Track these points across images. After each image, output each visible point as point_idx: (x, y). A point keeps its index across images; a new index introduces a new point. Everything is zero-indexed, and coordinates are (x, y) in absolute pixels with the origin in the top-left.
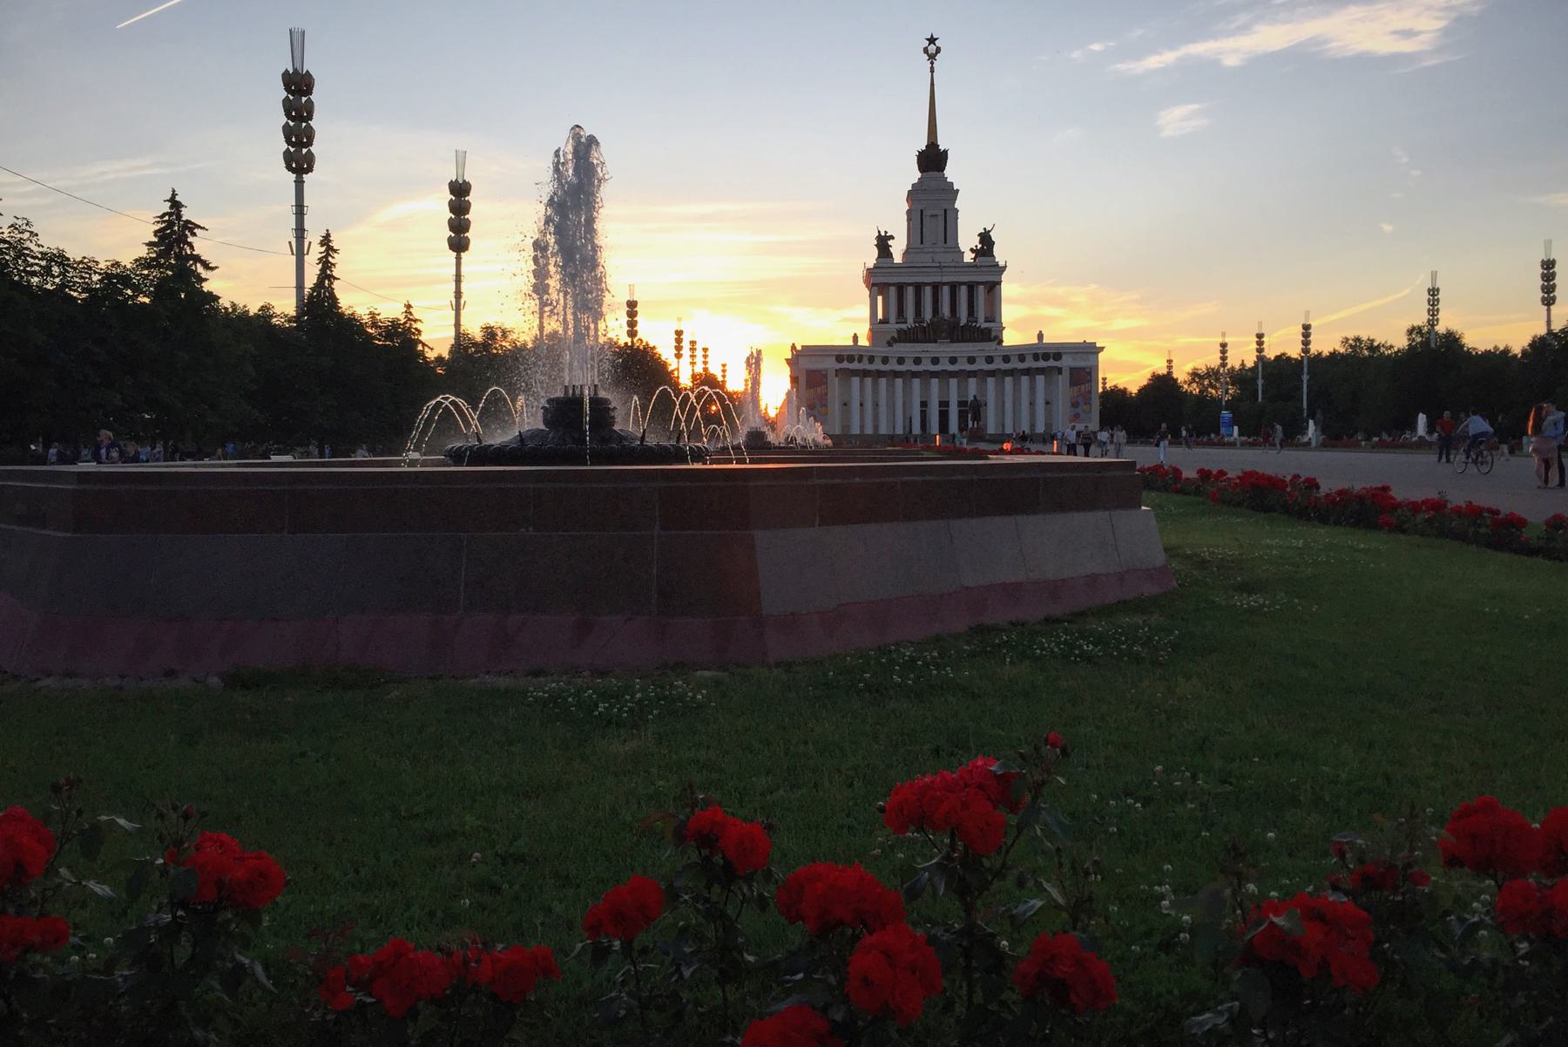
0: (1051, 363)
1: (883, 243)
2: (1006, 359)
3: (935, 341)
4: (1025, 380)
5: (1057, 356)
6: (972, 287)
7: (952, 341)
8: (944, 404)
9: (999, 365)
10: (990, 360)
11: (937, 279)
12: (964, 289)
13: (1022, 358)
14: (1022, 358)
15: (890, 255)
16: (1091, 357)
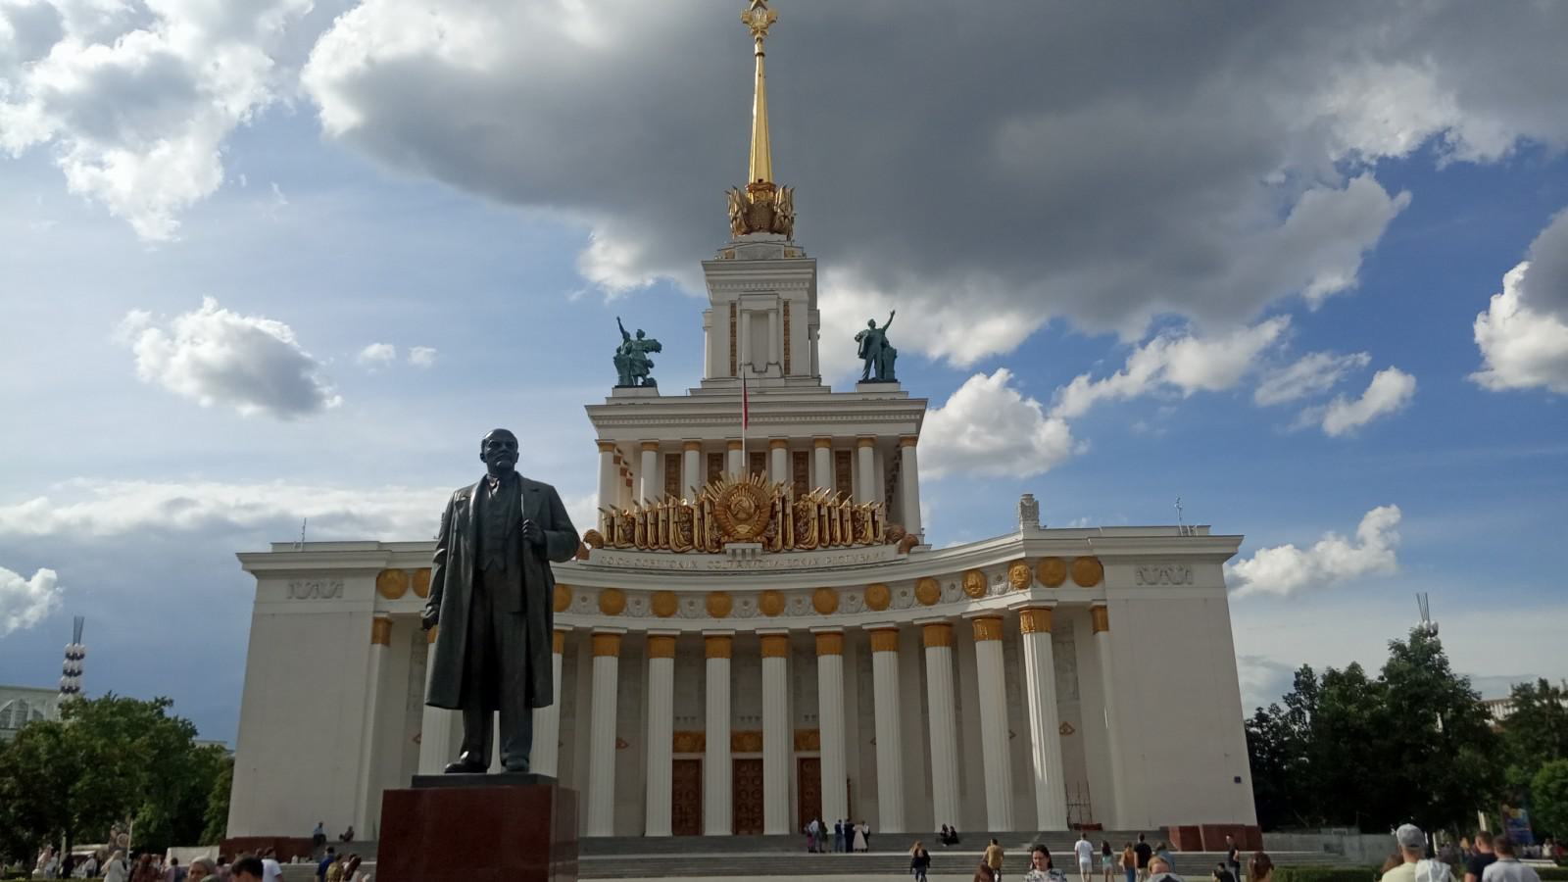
0: (1070, 593)
1: (634, 361)
2: (928, 590)
3: (718, 546)
4: (988, 654)
5: (1090, 571)
6: (844, 457)
7: (769, 545)
8: (746, 739)
9: (904, 613)
10: (878, 597)
11: (760, 433)
12: (822, 458)
13: (979, 581)
14: (979, 581)
15: (652, 383)
16: (1201, 572)
